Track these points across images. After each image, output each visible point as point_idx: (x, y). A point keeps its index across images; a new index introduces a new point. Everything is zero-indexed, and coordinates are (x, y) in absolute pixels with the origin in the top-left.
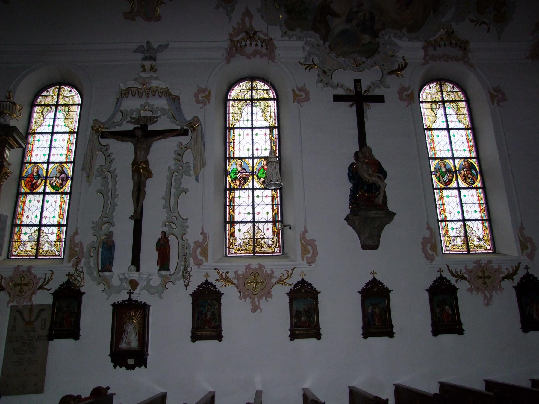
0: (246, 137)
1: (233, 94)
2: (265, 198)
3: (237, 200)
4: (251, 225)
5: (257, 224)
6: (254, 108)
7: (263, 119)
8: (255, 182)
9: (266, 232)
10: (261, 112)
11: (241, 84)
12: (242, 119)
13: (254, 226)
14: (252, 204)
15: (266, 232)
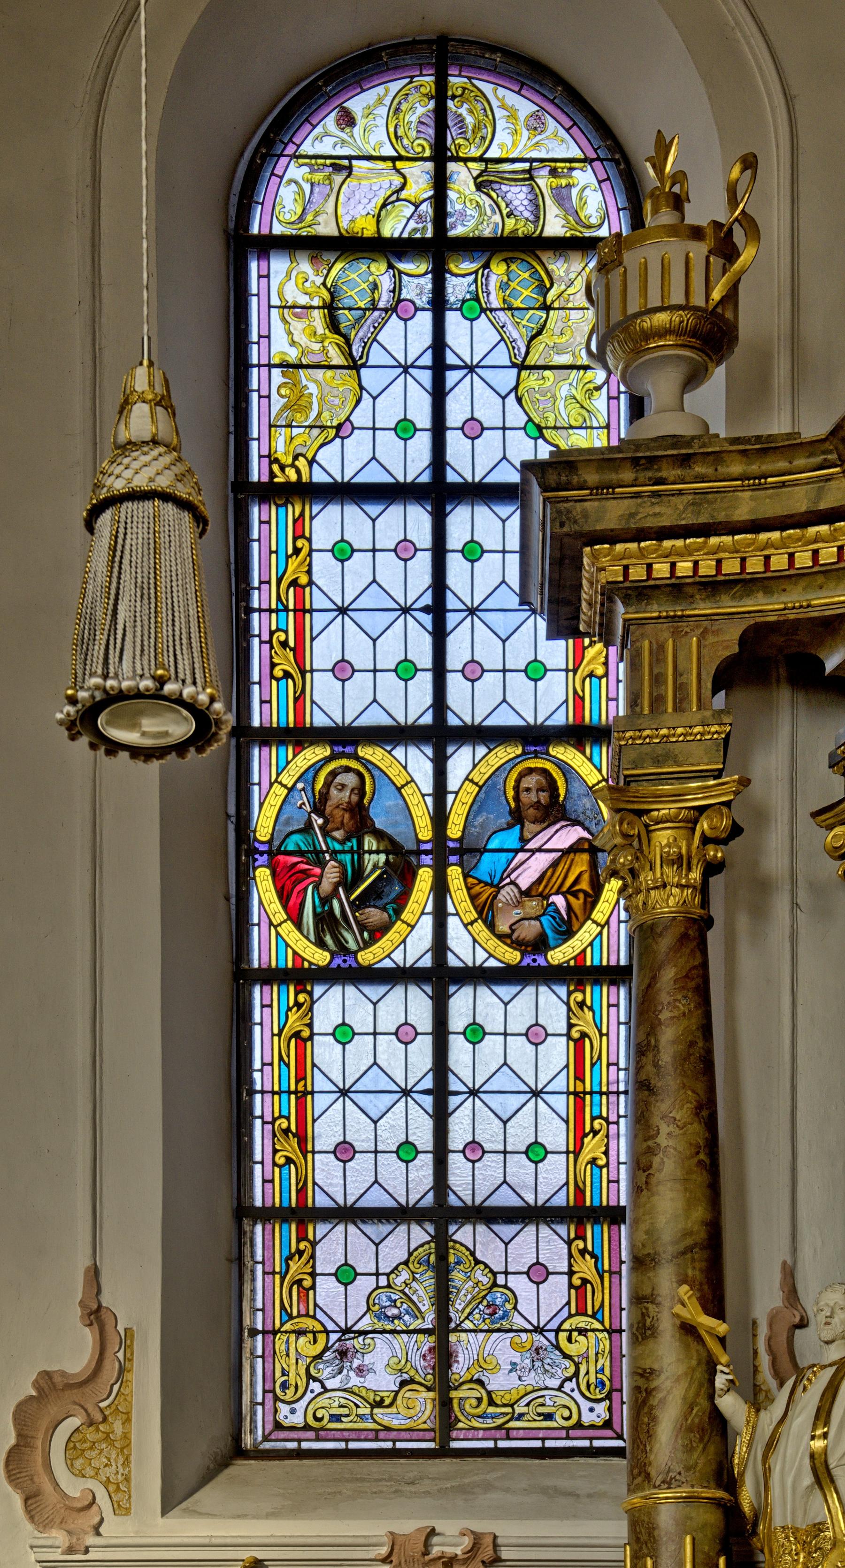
0: (389, 568)
1: (288, 200)
2: (519, 1048)
3: (325, 1052)
4: (420, 1234)
5: (463, 1234)
6: (452, 318)
7: (516, 416)
8: (453, 925)
9: (521, 1285)
10: (501, 356)
11: (357, 105)
12: (361, 417)
13: (442, 1242)
14: (428, 1083)
15: (521, 1285)
